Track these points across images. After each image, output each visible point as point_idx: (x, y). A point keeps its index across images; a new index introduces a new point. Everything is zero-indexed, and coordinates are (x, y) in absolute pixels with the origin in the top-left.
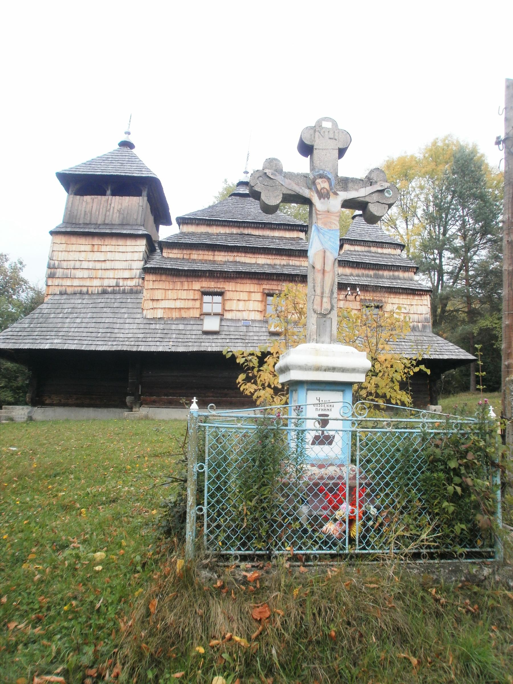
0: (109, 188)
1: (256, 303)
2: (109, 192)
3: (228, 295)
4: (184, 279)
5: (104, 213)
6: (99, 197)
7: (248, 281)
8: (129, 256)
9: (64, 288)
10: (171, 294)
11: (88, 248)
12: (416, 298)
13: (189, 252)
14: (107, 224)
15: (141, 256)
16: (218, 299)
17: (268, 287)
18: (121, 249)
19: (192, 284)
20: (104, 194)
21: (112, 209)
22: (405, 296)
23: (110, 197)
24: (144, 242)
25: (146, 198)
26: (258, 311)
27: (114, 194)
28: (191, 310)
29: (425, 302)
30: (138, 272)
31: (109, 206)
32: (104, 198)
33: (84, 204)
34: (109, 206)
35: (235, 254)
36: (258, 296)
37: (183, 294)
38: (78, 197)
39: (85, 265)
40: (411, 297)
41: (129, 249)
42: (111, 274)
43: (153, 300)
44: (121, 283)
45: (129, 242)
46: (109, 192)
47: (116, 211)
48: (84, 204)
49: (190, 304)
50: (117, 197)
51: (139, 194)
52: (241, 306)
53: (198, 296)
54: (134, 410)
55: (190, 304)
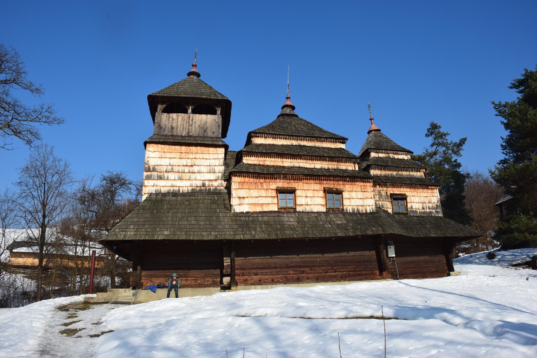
0: (190, 107)
1: (320, 199)
2: (190, 111)
3: (298, 193)
4: (262, 180)
5: (187, 127)
6: (183, 114)
7: (312, 181)
8: (213, 162)
9: (159, 188)
10: (254, 193)
11: (178, 155)
12: (429, 191)
13: (263, 159)
14: (191, 136)
15: (222, 162)
16: (291, 196)
17: (327, 186)
18: (206, 156)
19: (269, 185)
20: (186, 112)
21: (194, 124)
22: (421, 190)
23: (191, 115)
24: (222, 150)
25: (220, 116)
26: (321, 205)
27: (194, 112)
28: (271, 205)
29: (436, 194)
30: (220, 175)
31: (191, 121)
32: (186, 116)
33: (171, 119)
34: (191, 121)
35: (299, 161)
36: (321, 194)
37: (263, 193)
38: (165, 114)
39: (176, 169)
40: (425, 190)
41: (211, 156)
42: (198, 176)
43: (239, 198)
44: (207, 183)
45: (211, 150)
46: (190, 111)
47: (197, 126)
48: (171, 119)
49: (269, 200)
50: (197, 115)
51: (214, 113)
52: (309, 201)
53: (274, 194)
54: (232, 288)
55: (269, 200)
